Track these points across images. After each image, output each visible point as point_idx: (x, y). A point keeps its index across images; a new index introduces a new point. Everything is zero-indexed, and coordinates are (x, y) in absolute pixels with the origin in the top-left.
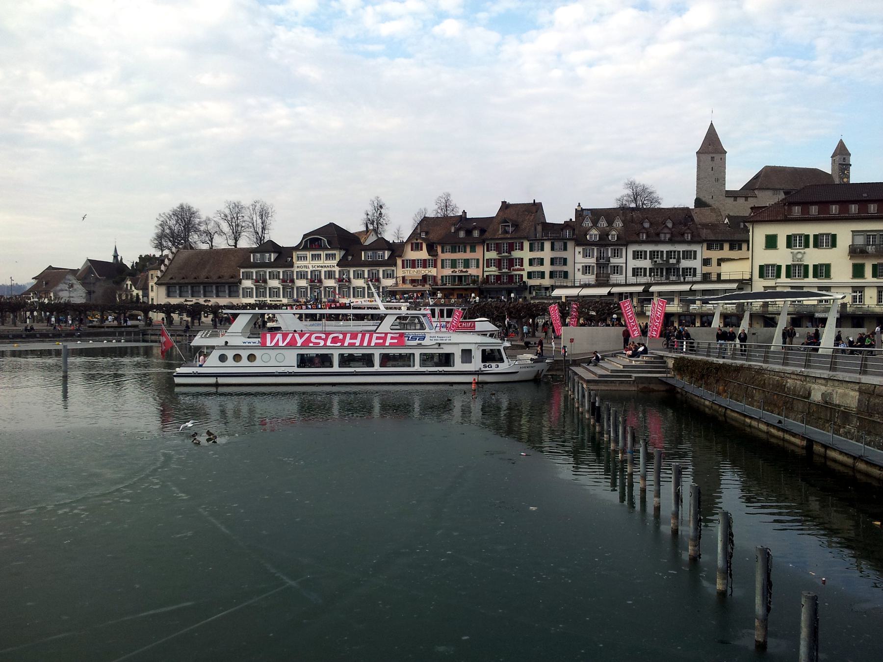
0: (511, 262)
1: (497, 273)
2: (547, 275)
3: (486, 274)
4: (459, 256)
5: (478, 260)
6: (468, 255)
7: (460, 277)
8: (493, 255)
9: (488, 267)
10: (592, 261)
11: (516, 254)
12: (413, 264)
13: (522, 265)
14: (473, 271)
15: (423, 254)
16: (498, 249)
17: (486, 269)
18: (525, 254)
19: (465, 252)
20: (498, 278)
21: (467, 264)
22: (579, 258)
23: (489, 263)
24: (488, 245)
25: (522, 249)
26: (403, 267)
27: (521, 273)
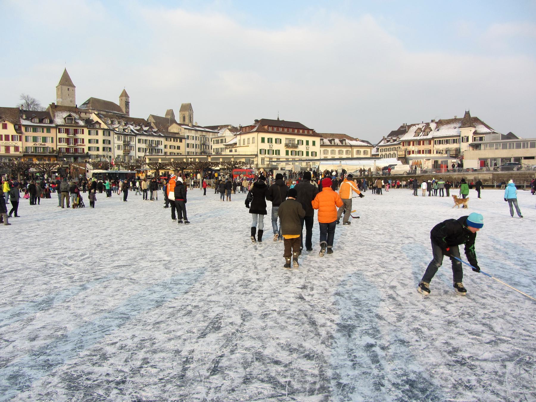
0: (76, 141)
1: (67, 147)
8: (64, 135)
9: (60, 142)
10: (121, 143)
11: (79, 136)
13: (83, 142)
16: (67, 131)
18: (85, 136)
20: (68, 150)
22: (116, 140)
23: (60, 140)
24: (59, 129)
25: (83, 133)
27: (83, 147)
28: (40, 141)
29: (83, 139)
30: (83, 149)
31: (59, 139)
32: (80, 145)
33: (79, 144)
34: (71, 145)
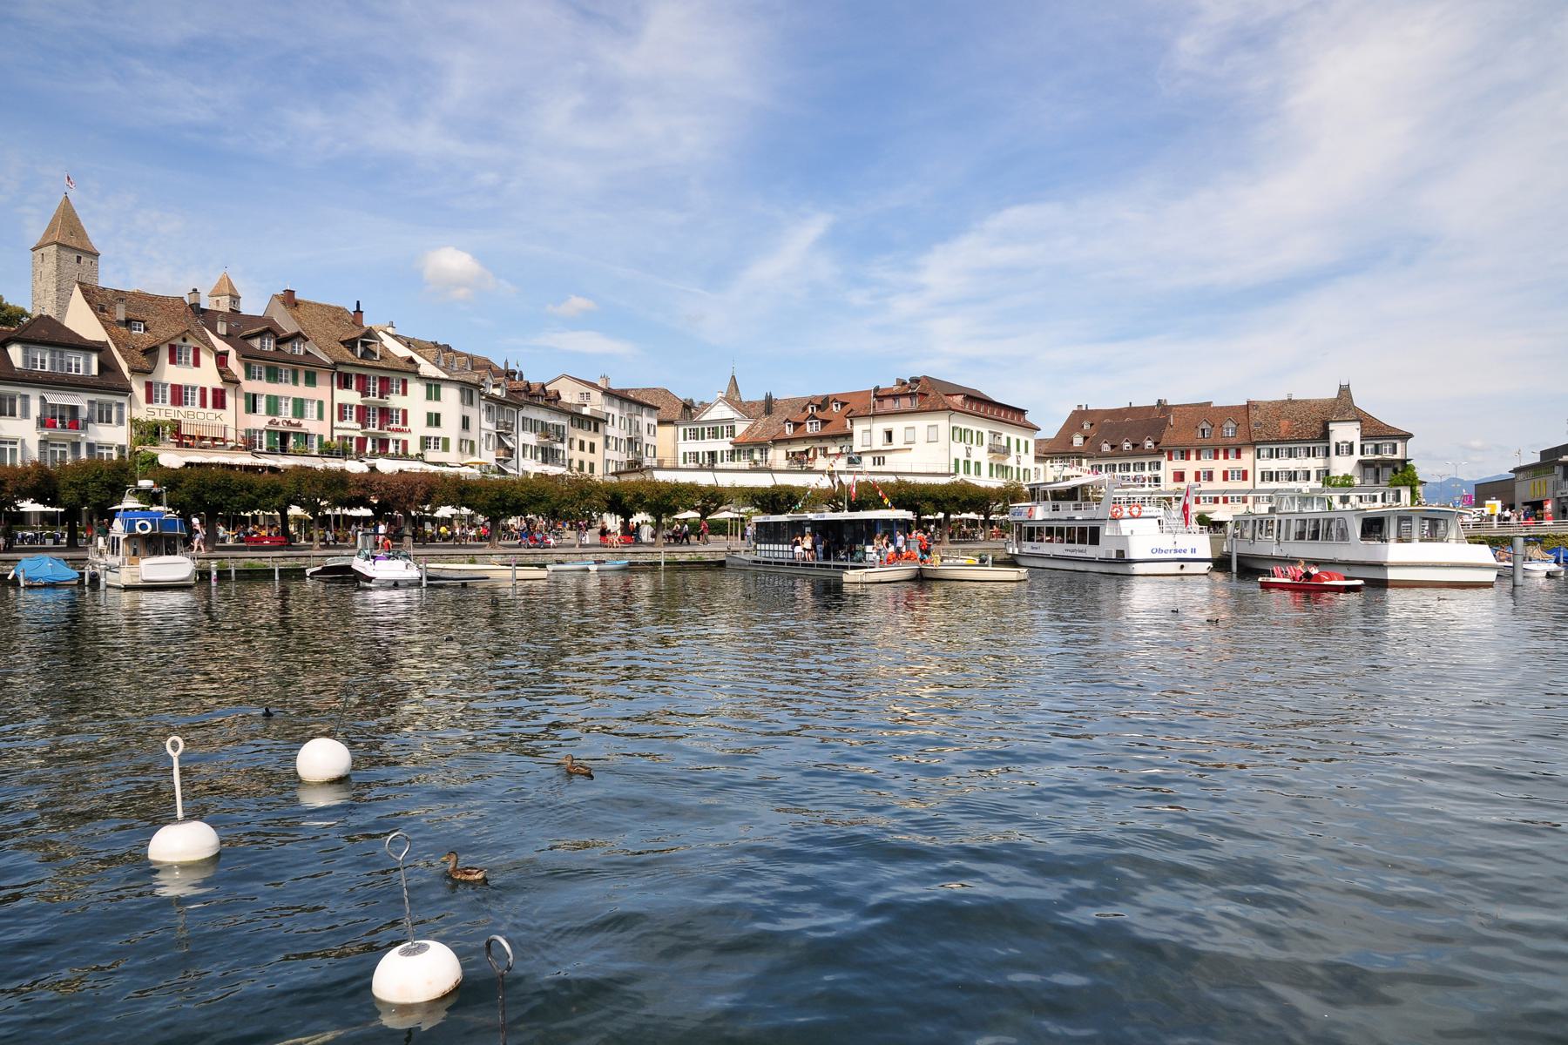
0: (385, 414)
1: (359, 434)
2: (453, 445)
3: (337, 433)
4: (286, 390)
5: (321, 403)
6: (301, 391)
7: (284, 436)
8: (352, 397)
11: (395, 401)
12: (179, 395)
13: (405, 422)
14: (310, 424)
15: (206, 375)
17: (337, 423)
19: (295, 381)
21: (299, 407)
26: (149, 400)
28: (287, 412)
29: (405, 412)
30: (405, 443)
31: (340, 405)
32: (398, 430)
33: (393, 426)
34: (370, 429)
